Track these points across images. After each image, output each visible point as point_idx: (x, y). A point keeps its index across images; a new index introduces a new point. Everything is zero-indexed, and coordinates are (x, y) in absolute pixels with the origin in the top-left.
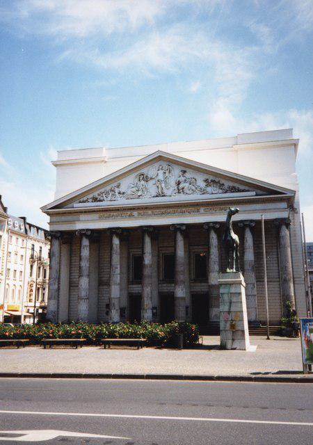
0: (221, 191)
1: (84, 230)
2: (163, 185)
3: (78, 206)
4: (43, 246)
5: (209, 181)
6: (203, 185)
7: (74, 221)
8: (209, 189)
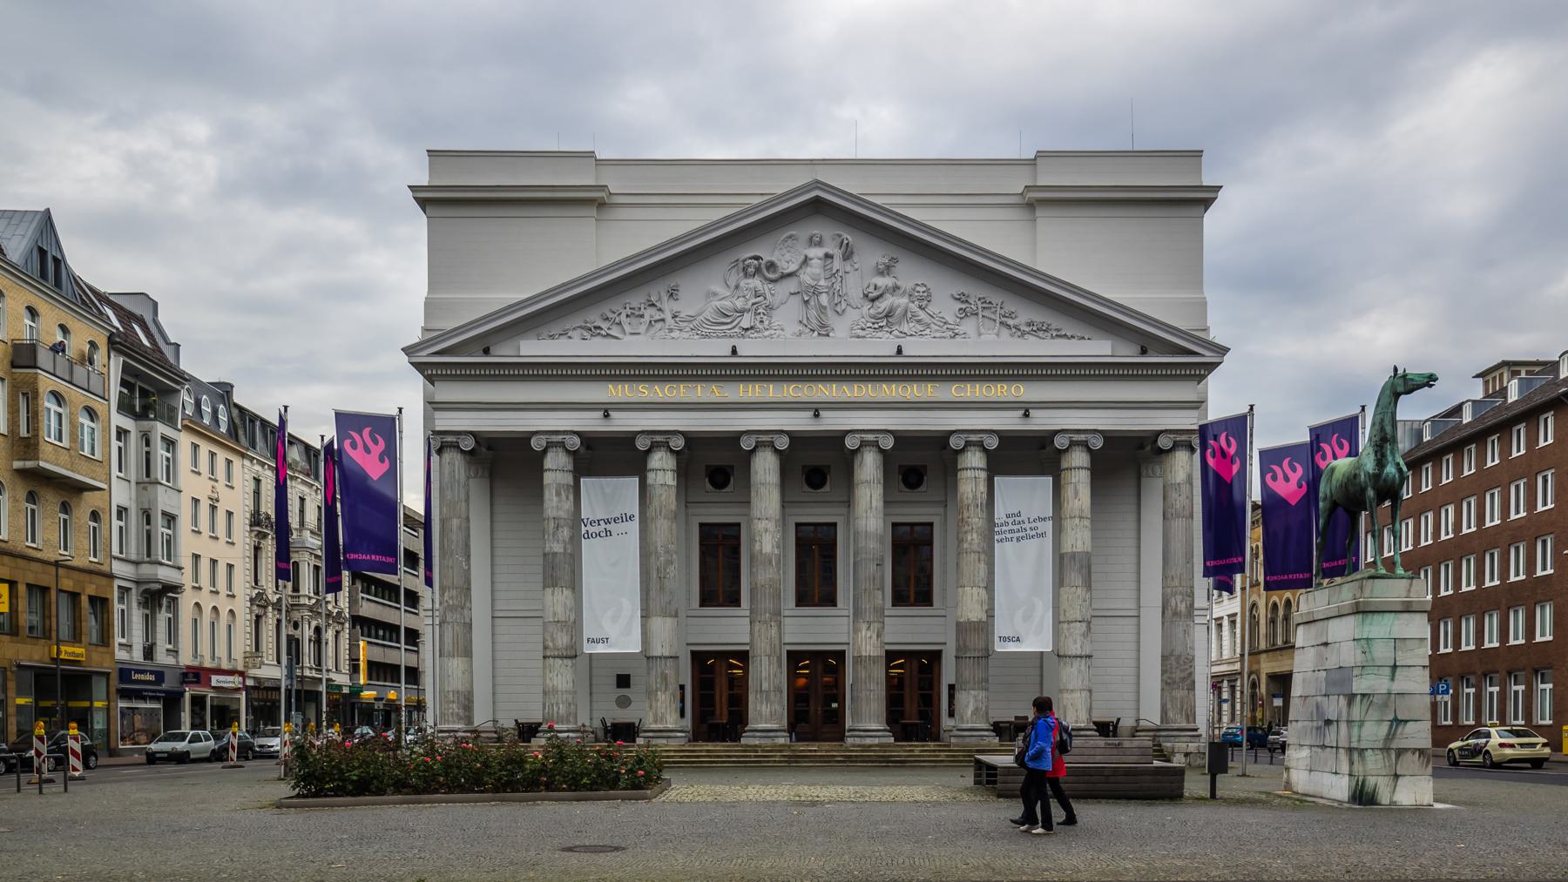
2: (824, 299)
3: (533, 348)
8: (969, 326)
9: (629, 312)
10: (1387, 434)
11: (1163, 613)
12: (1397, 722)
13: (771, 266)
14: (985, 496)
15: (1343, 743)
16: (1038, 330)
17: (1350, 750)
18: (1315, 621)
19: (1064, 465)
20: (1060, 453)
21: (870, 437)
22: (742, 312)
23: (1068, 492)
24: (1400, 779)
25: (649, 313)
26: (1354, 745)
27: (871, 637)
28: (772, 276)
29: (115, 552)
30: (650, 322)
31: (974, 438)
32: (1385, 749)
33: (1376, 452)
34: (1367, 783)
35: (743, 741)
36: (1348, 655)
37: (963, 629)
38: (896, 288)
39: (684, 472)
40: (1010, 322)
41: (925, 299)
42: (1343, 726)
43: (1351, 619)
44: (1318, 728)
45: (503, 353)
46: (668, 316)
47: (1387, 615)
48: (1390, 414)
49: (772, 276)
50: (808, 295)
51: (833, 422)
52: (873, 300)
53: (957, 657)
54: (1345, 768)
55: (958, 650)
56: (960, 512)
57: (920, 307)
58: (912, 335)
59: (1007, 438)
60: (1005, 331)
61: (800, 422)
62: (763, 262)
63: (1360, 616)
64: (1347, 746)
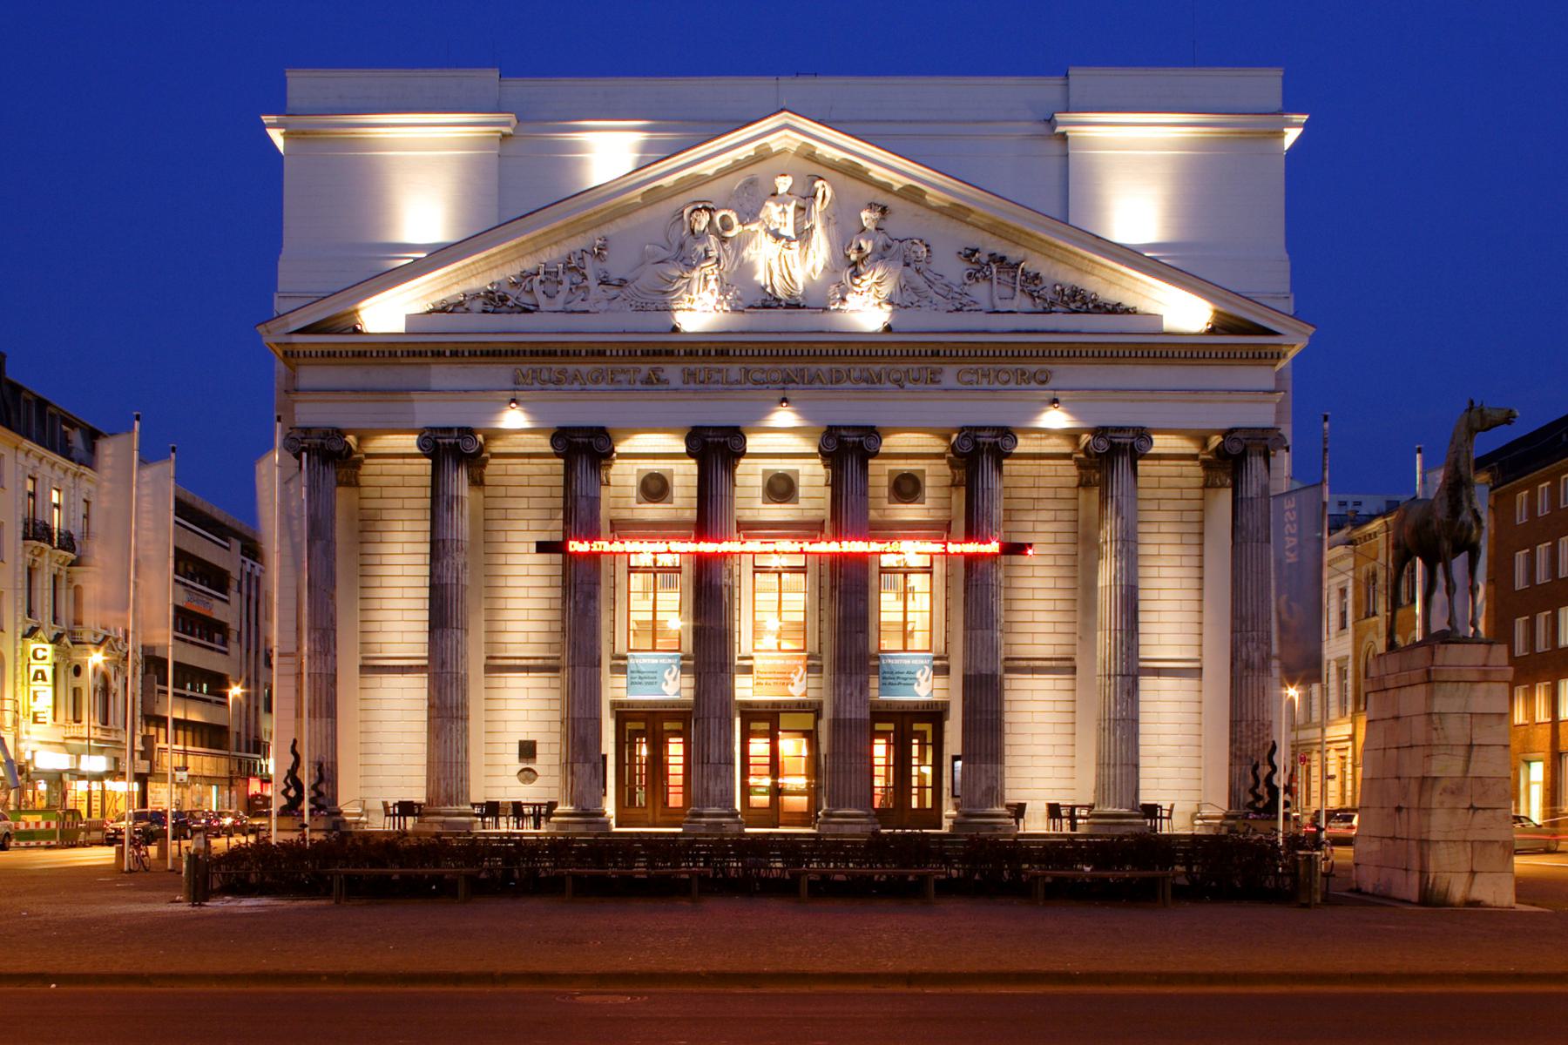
0: (1026, 303)
1: (448, 430)
5: (985, 259)
6: (955, 270)
7: (408, 391)
8: (980, 291)
10: (1461, 476)
26: (1424, 837)
27: (851, 695)
30: (571, 289)
33: (1450, 497)
34: (1438, 881)
43: (1424, 686)
46: (592, 282)
48: (1465, 454)
57: (918, 271)
58: (906, 307)
64: (1417, 838)
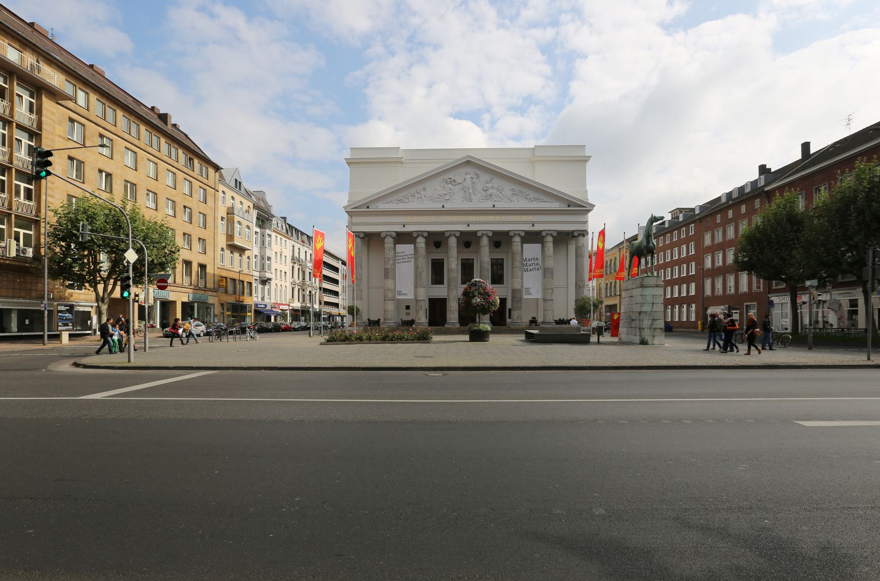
2: (471, 191)
3: (382, 206)
4: (301, 247)
8: (515, 198)
9: (411, 195)
11: (576, 286)
12: (654, 320)
13: (454, 181)
14: (520, 250)
15: (638, 326)
16: (536, 200)
17: (640, 328)
18: (628, 290)
19: (545, 241)
20: (543, 237)
21: (485, 232)
22: (446, 195)
23: (546, 249)
24: (655, 337)
25: (417, 195)
26: (641, 327)
28: (454, 184)
29: (254, 269)
31: (517, 233)
32: (650, 328)
35: (445, 326)
36: (639, 300)
37: (514, 291)
38: (493, 187)
39: (427, 244)
40: (528, 197)
41: (500, 190)
42: (638, 321)
43: (640, 289)
44: (630, 322)
45: (372, 208)
47: (650, 288)
49: (454, 184)
50: (465, 190)
51: (473, 228)
52: (486, 191)
53: (512, 300)
54: (638, 333)
55: (512, 298)
56: (513, 255)
59: (527, 233)
60: (526, 200)
61: (463, 228)
62: (452, 180)
63: (642, 288)
